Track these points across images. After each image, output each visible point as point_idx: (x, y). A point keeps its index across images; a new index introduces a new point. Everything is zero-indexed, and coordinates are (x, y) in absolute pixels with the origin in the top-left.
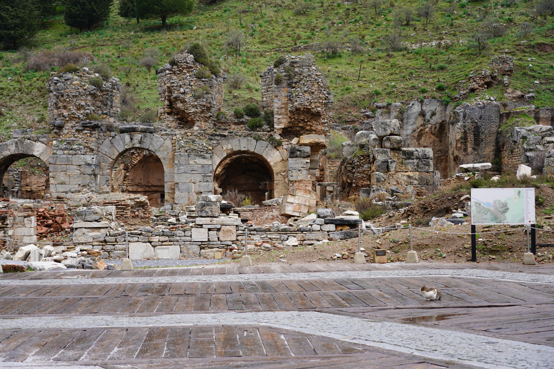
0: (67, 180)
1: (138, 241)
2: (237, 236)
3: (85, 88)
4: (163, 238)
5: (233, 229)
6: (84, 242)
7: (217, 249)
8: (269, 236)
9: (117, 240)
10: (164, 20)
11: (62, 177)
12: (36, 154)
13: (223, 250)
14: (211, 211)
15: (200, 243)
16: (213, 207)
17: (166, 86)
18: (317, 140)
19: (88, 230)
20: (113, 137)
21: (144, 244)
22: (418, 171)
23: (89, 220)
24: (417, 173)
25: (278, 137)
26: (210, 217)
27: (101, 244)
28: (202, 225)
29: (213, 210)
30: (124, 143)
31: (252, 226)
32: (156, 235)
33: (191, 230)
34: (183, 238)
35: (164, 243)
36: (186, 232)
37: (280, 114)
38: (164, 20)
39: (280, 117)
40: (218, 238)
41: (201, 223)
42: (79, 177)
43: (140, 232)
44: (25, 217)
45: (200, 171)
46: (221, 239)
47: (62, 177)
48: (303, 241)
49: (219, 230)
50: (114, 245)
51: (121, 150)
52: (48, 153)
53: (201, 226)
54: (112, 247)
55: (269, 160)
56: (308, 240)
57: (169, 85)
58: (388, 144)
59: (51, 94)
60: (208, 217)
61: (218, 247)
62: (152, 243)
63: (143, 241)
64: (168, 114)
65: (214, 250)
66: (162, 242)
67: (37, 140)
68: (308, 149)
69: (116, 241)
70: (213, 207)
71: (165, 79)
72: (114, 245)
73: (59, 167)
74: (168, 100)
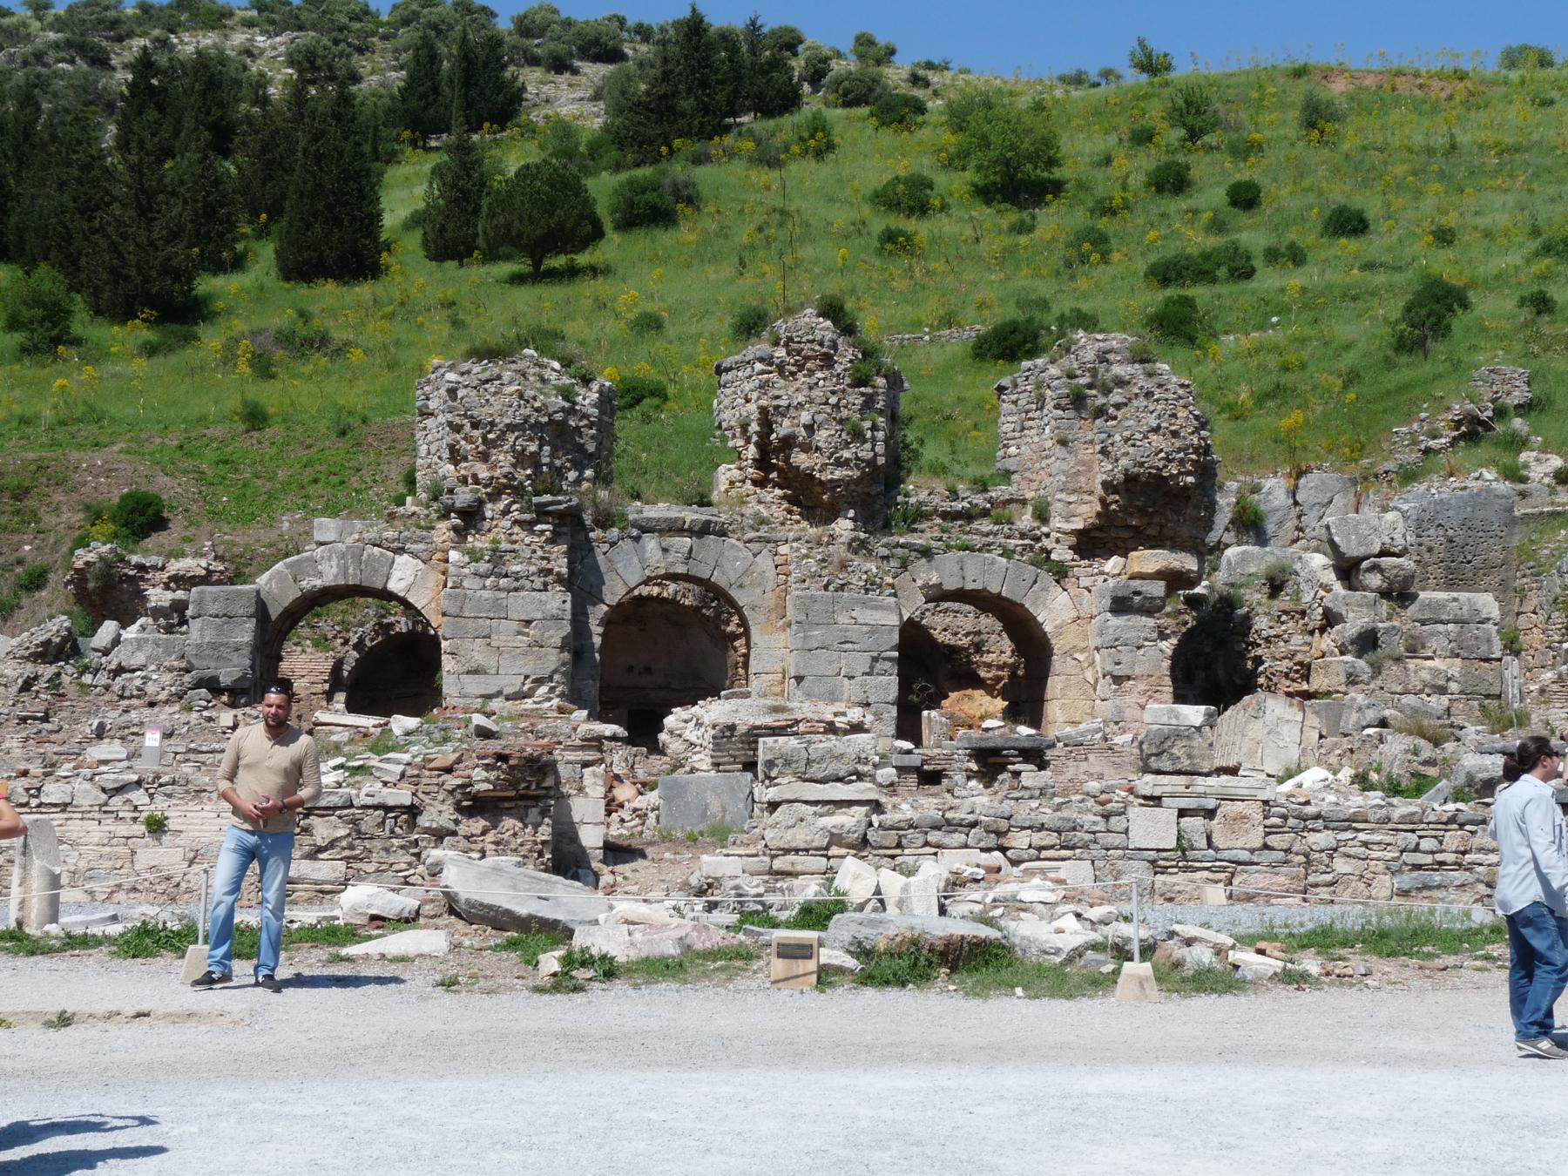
0: (489, 662)
1: (966, 846)
3: (537, 404)
4: (1039, 838)
5: (1254, 811)
6: (803, 846)
7: (1205, 874)
8: (1362, 836)
9: (904, 841)
10: (537, 264)
11: (477, 653)
12: (394, 586)
13: (1222, 876)
14: (1190, 756)
16: (1194, 743)
17: (752, 407)
18: (1176, 565)
19: (817, 809)
20: (613, 544)
22: (1458, 656)
24: (1458, 661)
25: (1062, 554)
28: (1159, 798)
29: (1196, 752)
31: (1307, 803)
32: (1023, 828)
35: (1044, 854)
36: (1113, 820)
37: (1074, 491)
38: (537, 264)
39: (1072, 498)
40: (1209, 838)
41: (1157, 793)
42: (525, 654)
43: (971, 818)
44: (586, 764)
45: (867, 643)
47: (477, 653)
48: (1464, 853)
49: (1210, 814)
50: (893, 857)
52: (431, 584)
53: (1155, 800)
55: (1040, 619)
56: (1480, 850)
57: (764, 402)
58: (1375, 580)
59: (430, 422)
60: (1178, 773)
62: (1009, 853)
63: (982, 844)
64: (755, 483)
65: (1199, 875)
66: (1040, 849)
67: (400, 551)
68: (1157, 589)
70: (1194, 743)
71: (748, 386)
72: (893, 857)
73: (470, 623)
74: (757, 444)
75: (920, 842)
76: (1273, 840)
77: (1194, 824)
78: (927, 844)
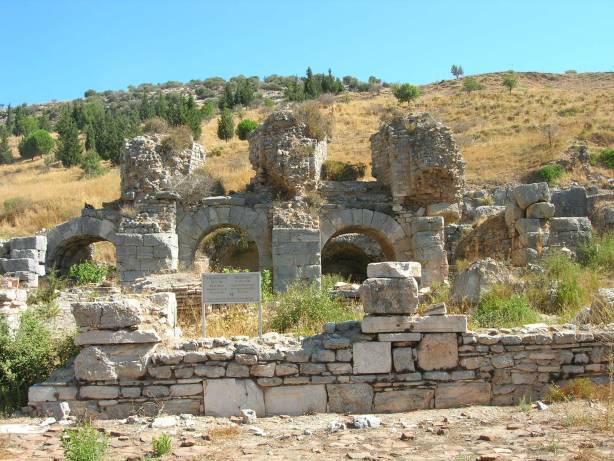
2: (460, 358)
14: (399, 301)
21: (242, 382)
23: (111, 325)
27: (138, 383)
35: (287, 381)
36: (340, 352)
46: (423, 364)
49: (415, 345)
53: (375, 337)
66: (282, 377)
76: (465, 362)
78: (194, 375)
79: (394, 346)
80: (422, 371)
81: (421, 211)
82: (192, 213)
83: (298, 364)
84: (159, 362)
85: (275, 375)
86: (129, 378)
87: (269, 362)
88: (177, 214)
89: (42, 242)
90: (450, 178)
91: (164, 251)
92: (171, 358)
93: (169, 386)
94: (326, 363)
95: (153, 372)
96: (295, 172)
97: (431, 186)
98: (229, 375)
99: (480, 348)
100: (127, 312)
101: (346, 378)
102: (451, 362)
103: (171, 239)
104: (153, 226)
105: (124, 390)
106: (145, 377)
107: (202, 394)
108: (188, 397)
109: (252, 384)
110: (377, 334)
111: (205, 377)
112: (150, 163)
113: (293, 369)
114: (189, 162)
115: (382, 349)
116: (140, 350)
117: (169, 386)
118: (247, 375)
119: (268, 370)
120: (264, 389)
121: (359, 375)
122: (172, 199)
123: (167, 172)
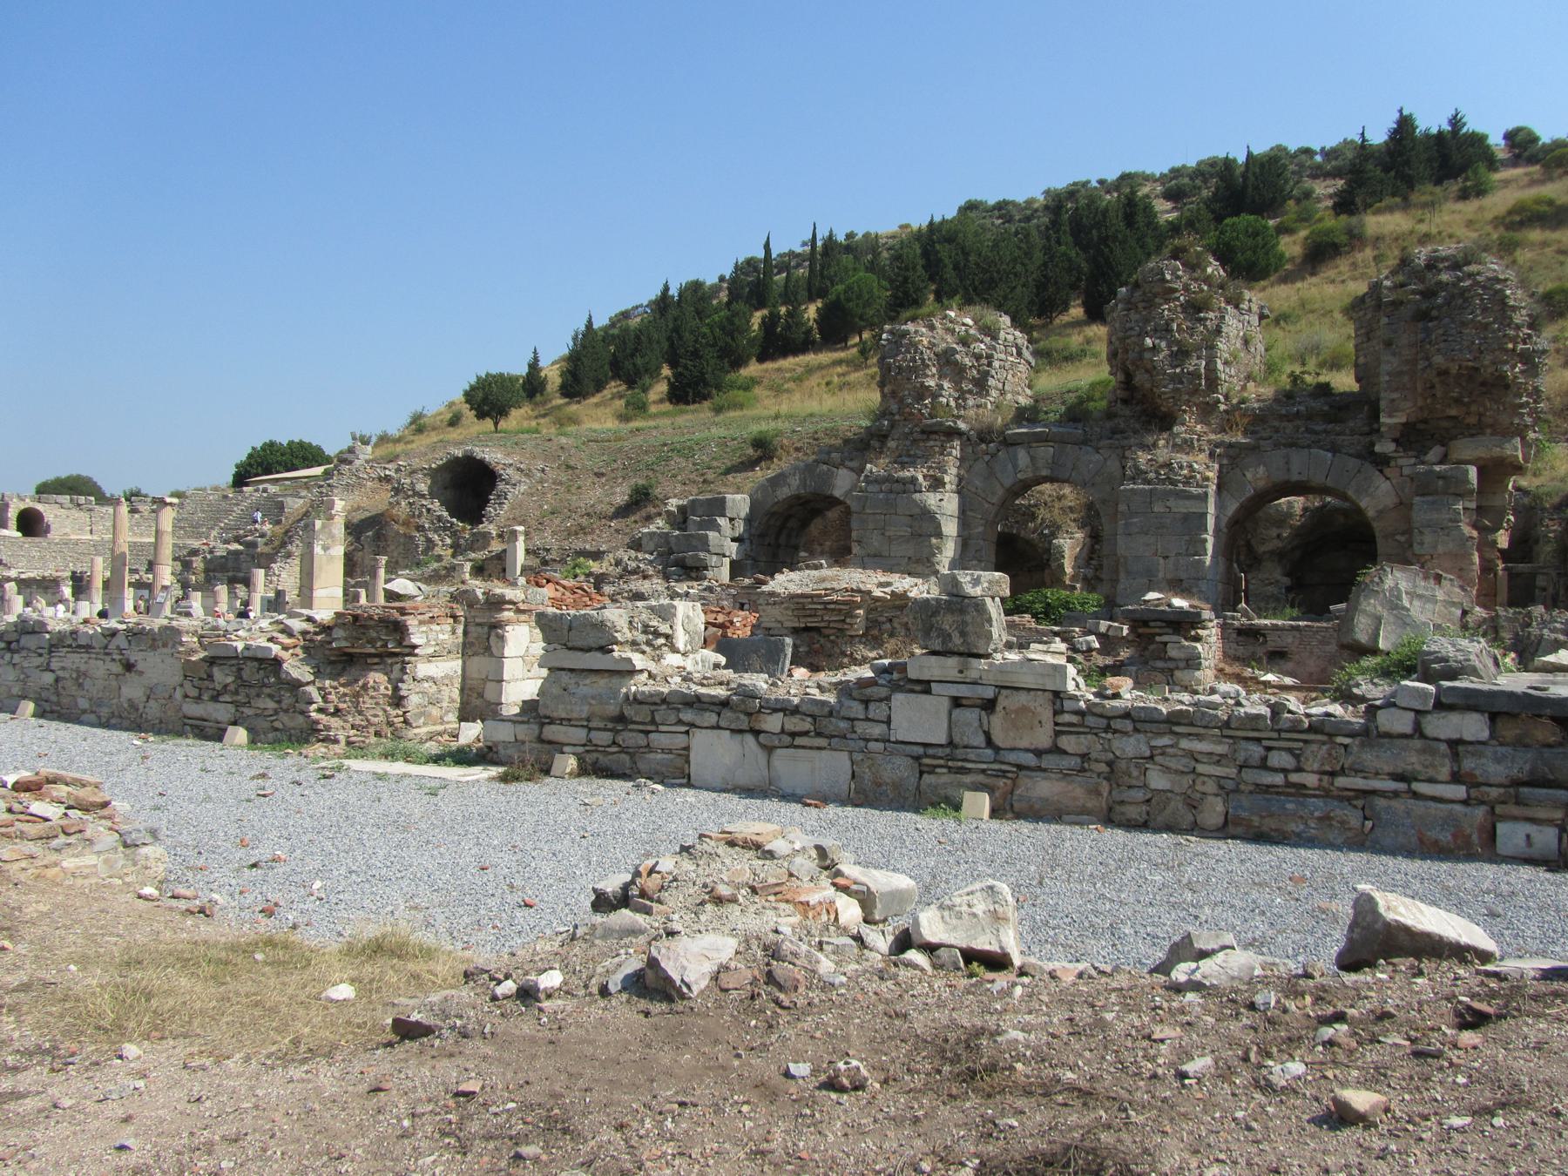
1: (718, 727)
2: (1057, 734)
9: (657, 718)
12: (837, 493)
13: (1001, 782)
14: (963, 634)
15: (920, 750)
16: (968, 618)
21: (738, 737)
23: (579, 644)
26: (961, 654)
27: (610, 726)
30: (1015, 466)
33: (888, 699)
34: (861, 727)
35: (799, 741)
36: (872, 706)
46: (999, 738)
49: (989, 706)
51: (1008, 482)
53: (925, 687)
54: (641, 740)
61: (983, 771)
66: (793, 735)
69: (653, 722)
70: (968, 618)
75: (673, 719)
76: (1067, 742)
77: (970, 716)
78: (680, 722)
79: (957, 702)
80: (997, 749)
81: (1434, 453)
82: (987, 458)
83: (814, 717)
84: (637, 700)
85: (783, 731)
86: (602, 718)
87: (775, 710)
88: (962, 459)
89: (739, 503)
90: (1502, 385)
91: (927, 524)
92: (651, 695)
93: (647, 733)
94: (853, 720)
95: (629, 712)
96: (1176, 379)
97: (1458, 401)
98: (722, 724)
99: (1090, 721)
100: (601, 626)
101: (880, 746)
102: (1043, 738)
103: (945, 505)
104: (914, 480)
105: (594, 734)
106: (621, 719)
107: (687, 748)
108: (670, 751)
109: (749, 738)
110: (929, 682)
111: (693, 725)
112: (914, 370)
113: (807, 725)
114: (990, 365)
115: (936, 705)
116: (615, 680)
117: (647, 733)
118: (745, 726)
119: (773, 723)
120: (769, 750)
121: (897, 742)
122: (953, 433)
123: (946, 385)
